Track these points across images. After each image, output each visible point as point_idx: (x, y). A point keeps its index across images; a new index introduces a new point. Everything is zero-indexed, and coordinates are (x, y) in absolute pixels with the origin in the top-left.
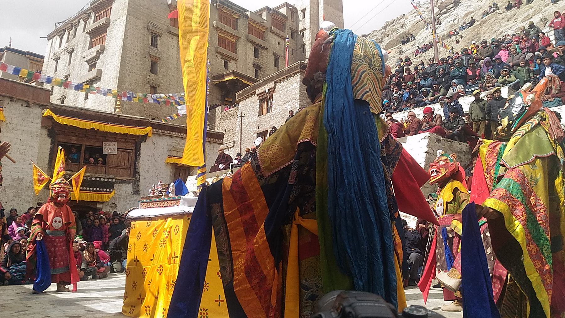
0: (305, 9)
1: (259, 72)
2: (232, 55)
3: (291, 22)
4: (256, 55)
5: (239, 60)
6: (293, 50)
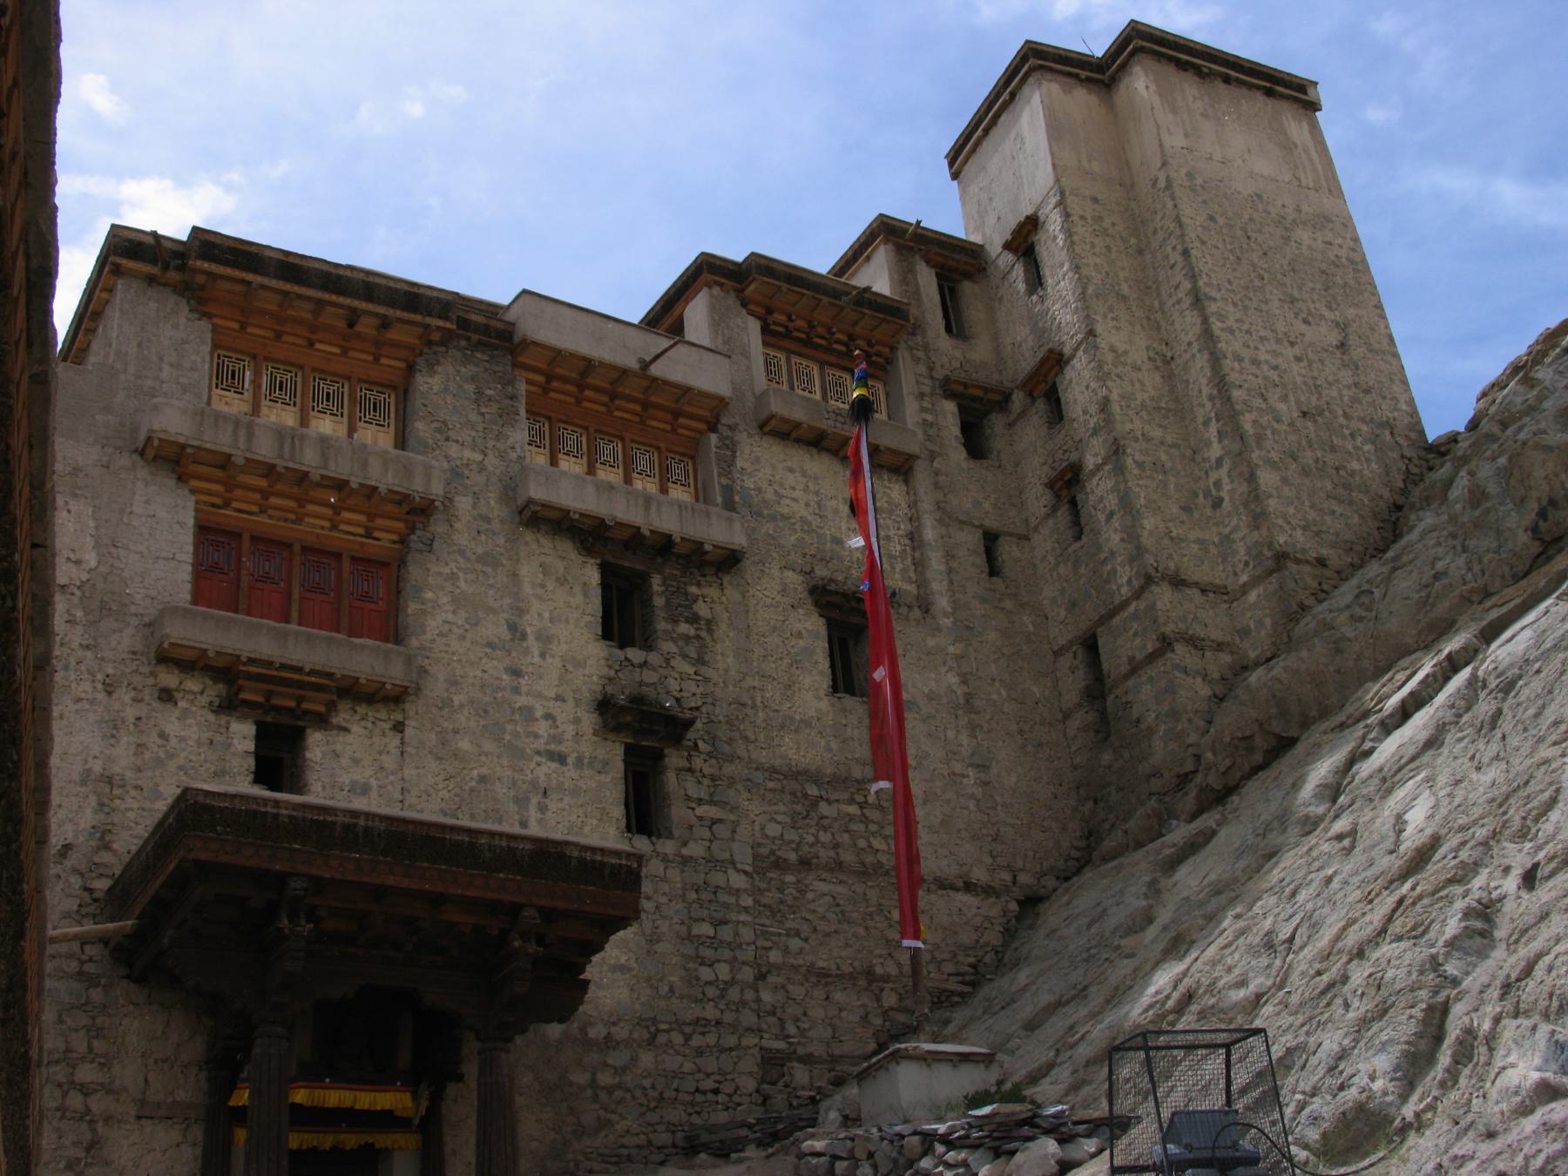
0: (1031, 224)
2: (361, 659)
3: (944, 342)
4: (623, 619)
5: (435, 689)
6: (990, 539)
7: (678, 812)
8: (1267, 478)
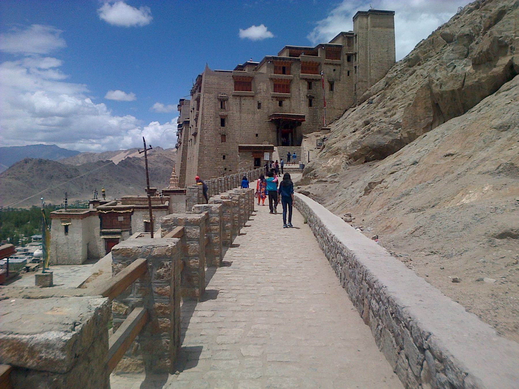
1: (313, 100)
7: (313, 104)
8: (372, 71)
